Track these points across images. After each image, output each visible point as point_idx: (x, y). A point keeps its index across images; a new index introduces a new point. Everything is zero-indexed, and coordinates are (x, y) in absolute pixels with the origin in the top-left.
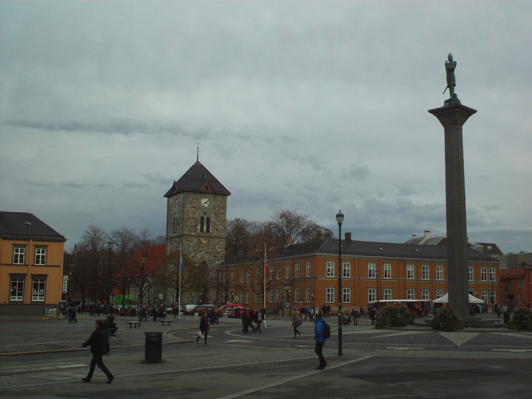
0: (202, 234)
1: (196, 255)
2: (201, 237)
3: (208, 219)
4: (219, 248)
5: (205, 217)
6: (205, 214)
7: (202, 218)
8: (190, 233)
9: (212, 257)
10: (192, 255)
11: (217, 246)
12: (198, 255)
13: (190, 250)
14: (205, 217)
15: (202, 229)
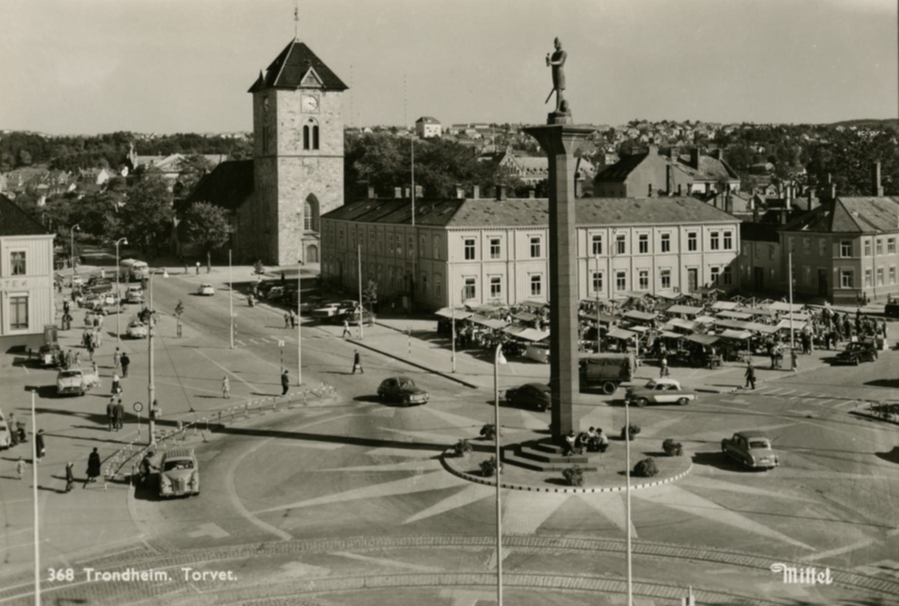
0: (306, 153)
1: (298, 186)
4: (335, 172)
5: (311, 126)
6: (311, 120)
7: (306, 129)
8: (288, 153)
9: (324, 186)
10: (293, 186)
11: (331, 171)
12: (301, 185)
13: (290, 179)
14: (311, 126)
15: (306, 146)
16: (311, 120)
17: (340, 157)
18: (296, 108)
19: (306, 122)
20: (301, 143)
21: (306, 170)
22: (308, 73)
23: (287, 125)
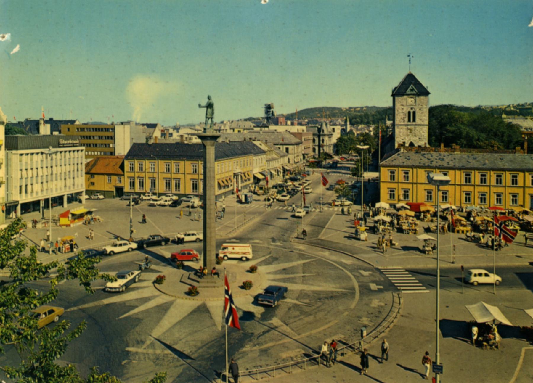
0: (409, 123)
2: (408, 125)
3: (414, 113)
4: (423, 132)
5: (412, 111)
6: (412, 109)
7: (409, 113)
8: (400, 123)
9: (417, 138)
11: (421, 132)
15: (409, 120)
16: (412, 109)
17: (426, 125)
18: (404, 103)
19: (409, 109)
20: (407, 119)
21: (409, 131)
22: (410, 88)
23: (400, 111)
